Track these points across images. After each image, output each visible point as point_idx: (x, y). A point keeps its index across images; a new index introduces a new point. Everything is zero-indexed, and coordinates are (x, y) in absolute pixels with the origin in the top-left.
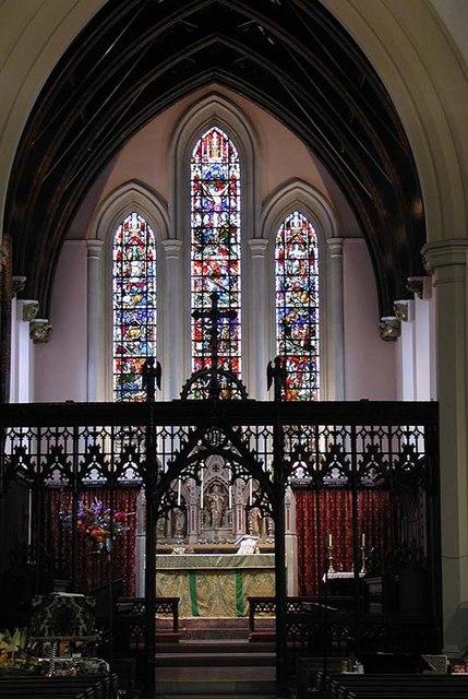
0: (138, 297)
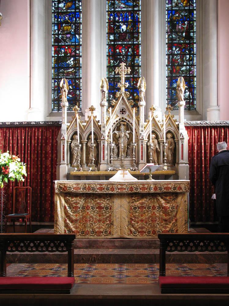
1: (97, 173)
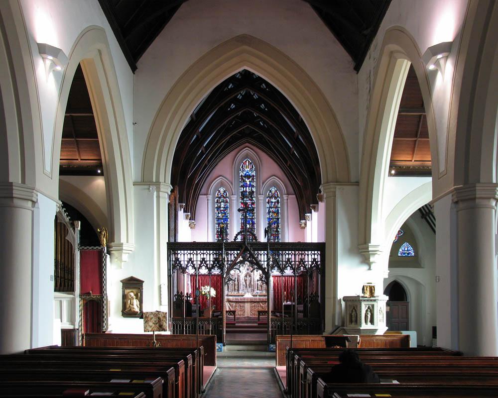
0: (223, 214)
1: (238, 294)
